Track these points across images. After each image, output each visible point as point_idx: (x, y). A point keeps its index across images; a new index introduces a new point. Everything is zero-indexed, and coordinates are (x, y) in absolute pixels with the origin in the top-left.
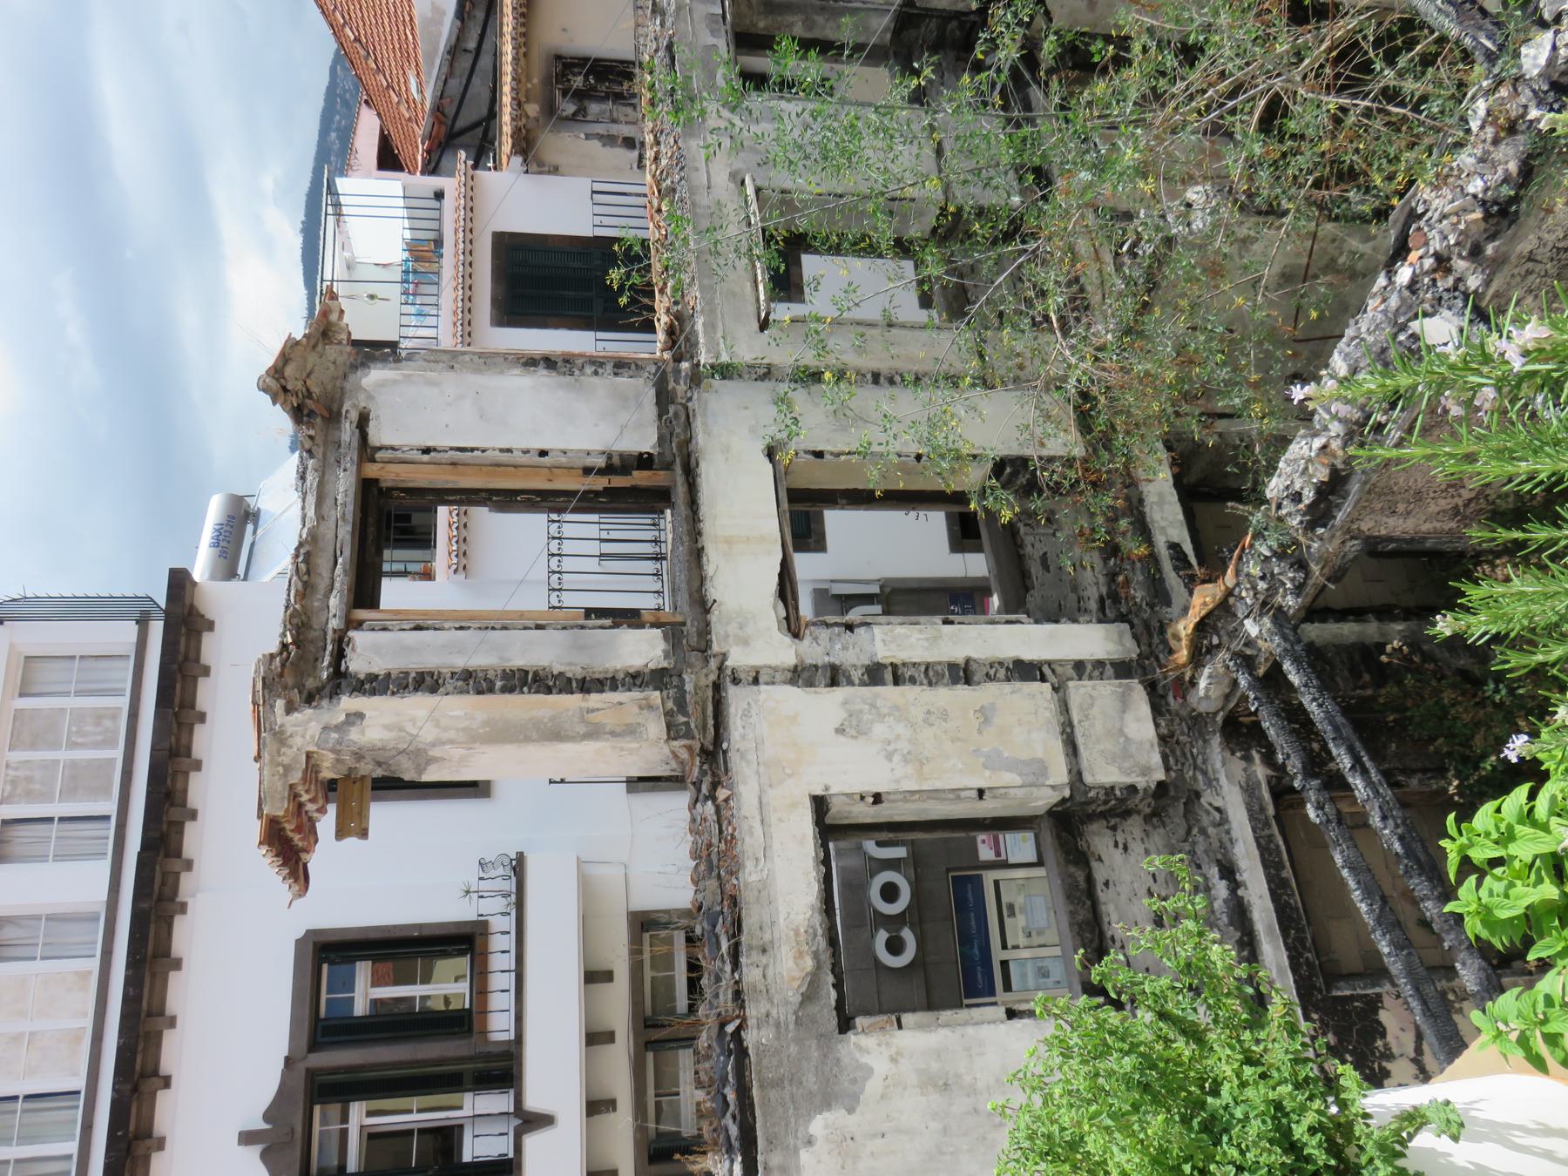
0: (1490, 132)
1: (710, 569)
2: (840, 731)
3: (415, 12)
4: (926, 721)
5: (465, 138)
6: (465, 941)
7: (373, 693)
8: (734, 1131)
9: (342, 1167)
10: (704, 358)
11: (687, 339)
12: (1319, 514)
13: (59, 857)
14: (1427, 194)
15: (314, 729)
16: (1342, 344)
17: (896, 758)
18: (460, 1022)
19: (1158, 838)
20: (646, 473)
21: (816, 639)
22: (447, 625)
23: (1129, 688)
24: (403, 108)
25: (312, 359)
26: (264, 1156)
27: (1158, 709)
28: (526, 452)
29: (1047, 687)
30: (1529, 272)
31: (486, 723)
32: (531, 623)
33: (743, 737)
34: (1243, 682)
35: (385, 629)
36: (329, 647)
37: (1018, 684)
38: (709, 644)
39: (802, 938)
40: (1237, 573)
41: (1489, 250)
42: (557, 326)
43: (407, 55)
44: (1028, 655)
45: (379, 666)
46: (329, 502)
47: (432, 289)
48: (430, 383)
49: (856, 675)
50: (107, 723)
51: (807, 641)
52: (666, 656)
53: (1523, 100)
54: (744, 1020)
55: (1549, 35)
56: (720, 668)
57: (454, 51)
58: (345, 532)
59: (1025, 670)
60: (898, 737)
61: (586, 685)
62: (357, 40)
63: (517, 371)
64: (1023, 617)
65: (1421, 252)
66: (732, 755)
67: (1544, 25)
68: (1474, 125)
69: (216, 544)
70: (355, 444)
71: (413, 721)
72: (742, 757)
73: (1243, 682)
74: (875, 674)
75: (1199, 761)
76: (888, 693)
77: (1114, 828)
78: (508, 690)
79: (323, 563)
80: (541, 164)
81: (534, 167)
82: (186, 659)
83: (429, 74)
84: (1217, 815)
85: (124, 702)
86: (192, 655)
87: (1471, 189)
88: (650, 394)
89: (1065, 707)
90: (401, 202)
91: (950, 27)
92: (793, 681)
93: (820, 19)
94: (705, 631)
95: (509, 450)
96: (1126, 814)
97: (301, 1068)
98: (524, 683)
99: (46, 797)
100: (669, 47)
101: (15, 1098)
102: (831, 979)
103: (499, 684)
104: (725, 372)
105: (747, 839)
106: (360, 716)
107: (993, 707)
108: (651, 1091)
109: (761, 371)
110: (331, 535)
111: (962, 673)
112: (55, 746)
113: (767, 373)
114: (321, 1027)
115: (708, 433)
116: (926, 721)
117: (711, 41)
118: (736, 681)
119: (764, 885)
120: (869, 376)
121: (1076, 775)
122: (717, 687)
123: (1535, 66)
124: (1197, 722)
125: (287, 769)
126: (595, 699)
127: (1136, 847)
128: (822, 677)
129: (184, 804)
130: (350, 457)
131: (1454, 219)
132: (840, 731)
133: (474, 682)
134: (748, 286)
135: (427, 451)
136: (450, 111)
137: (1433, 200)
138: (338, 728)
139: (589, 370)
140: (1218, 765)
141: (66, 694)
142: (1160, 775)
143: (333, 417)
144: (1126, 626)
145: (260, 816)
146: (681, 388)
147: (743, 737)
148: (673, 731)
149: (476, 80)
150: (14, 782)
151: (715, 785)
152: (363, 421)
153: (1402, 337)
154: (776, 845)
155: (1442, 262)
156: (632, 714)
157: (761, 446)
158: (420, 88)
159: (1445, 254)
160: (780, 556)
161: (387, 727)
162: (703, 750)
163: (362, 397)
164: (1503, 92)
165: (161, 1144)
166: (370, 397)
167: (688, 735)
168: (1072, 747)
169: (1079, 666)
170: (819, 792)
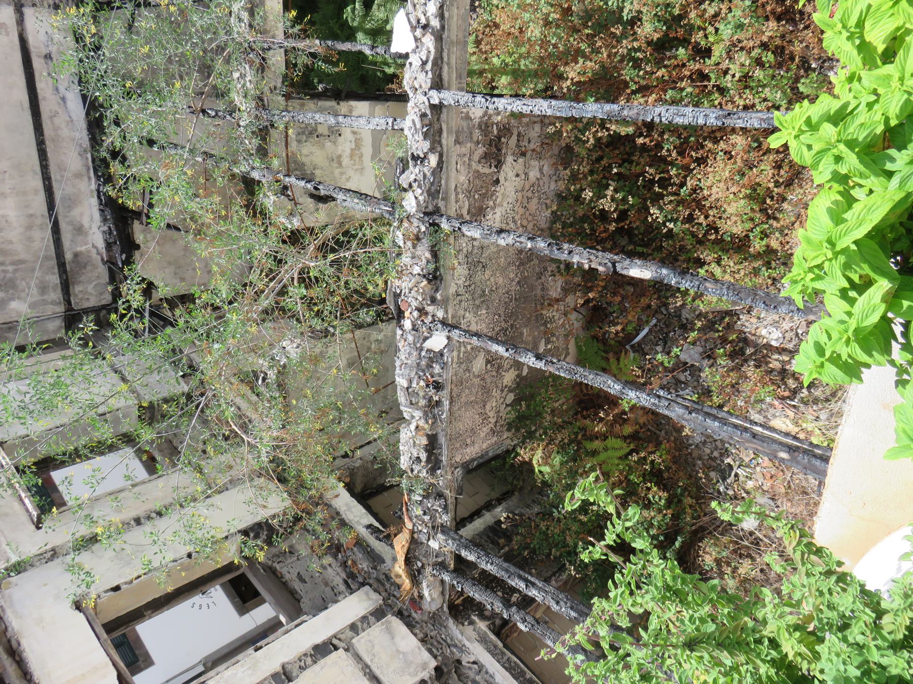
0: (409, 244)
12: (434, 464)
14: (397, 283)
16: (397, 371)
23: (389, 622)
27: (410, 624)
29: (341, 651)
30: (461, 301)
34: (447, 578)
40: (411, 519)
41: (438, 296)
44: (319, 639)
53: (416, 224)
55: (410, 193)
59: (323, 650)
64: (304, 617)
65: (409, 310)
67: (405, 190)
68: (401, 243)
73: (447, 578)
75: (449, 641)
84: (475, 666)
87: (415, 272)
89: (358, 658)
91: (101, 314)
109: (49, 555)
113: (54, 553)
120: (132, 522)
123: (412, 207)
124: (435, 618)
131: (416, 289)
134: (17, 506)
137: (403, 284)
140: (460, 636)
142: (433, 664)
144: (367, 587)
153: (423, 353)
155: (422, 311)
157: (68, 605)
159: (421, 307)
160: (115, 673)
164: (406, 224)
169: (353, 627)
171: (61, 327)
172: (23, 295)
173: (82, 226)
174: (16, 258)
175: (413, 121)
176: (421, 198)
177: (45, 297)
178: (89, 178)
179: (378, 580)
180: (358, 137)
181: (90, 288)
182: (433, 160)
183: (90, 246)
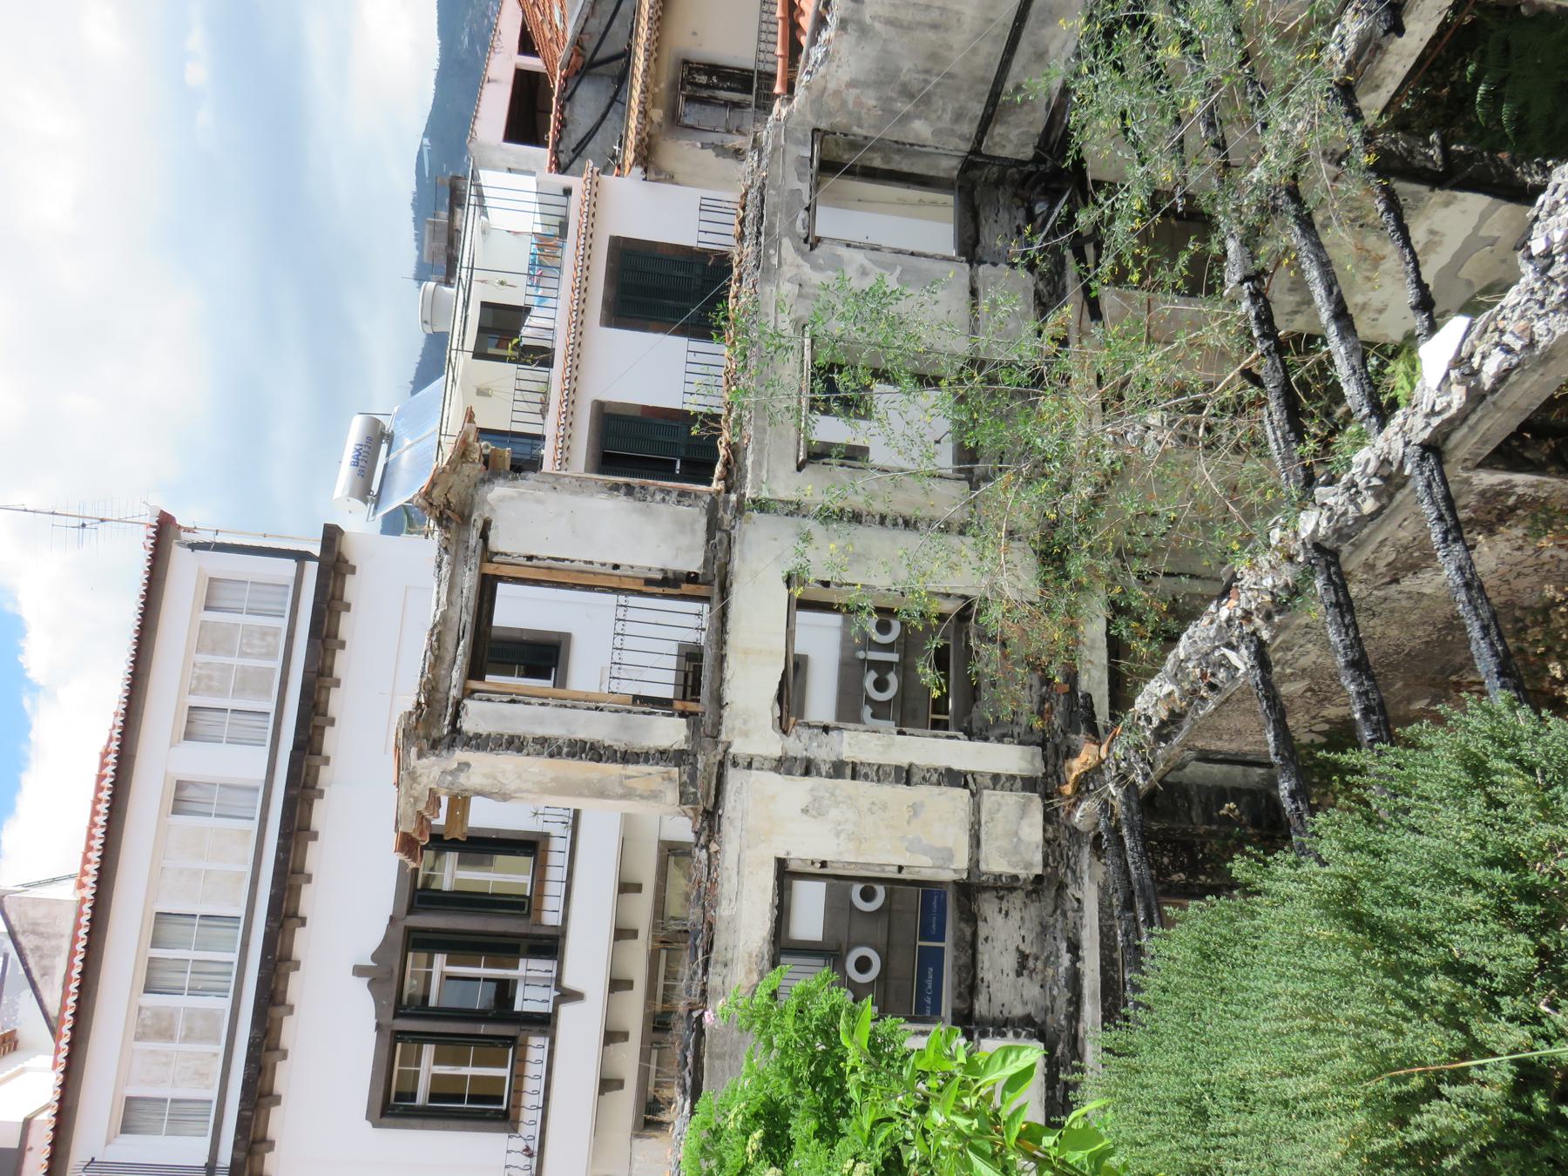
1: (728, 674)
2: (805, 811)
4: (870, 810)
5: (601, 69)
6: (530, 846)
7: (478, 748)
8: (689, 1081)
9: (426, 998)
10: (749, 493)
11: (740, 470)
12: (1163, 733)
15: (436, 772)
17: (843, 836)
18: (521, 905)
19: (1033, 910)
20: (692, 587)
24: (546, 27)
25: (454, 478)
26: (370, 985)
27: (1049, 817)
28: (603, 565)
31: (553, 780)
32: (592, 705)
33: (734, 808)
35: (489, 700)
36: (450, 710)
37: (944, 789)
38: (719, 732)
39: (754, 959)
40: (1109, 750)
41: (1277, 619)
42: (656, 331)
44: (957, 766)
45: (484, 729)
46: (457, 591)
48: (539, 501)
49: (824, 768)
50: (270, 639)
51: (791, 738)
52: (687, 741)
58: (467, 618)
59: (953, 778)
61: (628, 757)
63: (603, 496)
64: (960, 734)
69: (356, 464)
70: (479, 551)
72: (731, 823)
74: (839, 769)
76: (846, 785)
77: (1001, 898)
78: (571, 755)
80: (659, 171)
81: (652, 175)
82: (333, 598)
85: (284, 623)
86: (338, 593)
88: (703, 522)
89: (977, 809)
90: (534, 197)
92: (776, 770)
93: (897, 158)
95: (591, 563)
96: (1011, 889)
97: (401, 926)
98: (583, 750)
99: (222, 692)
101: (194, 916)
103: (565, 750)
104: (762, 506)
105: (726, 885)
106: (467, 765)
107: (922, 805)
109: (792, 508)
110: (456, 619)
111: (905, 776)
112: (230, 653)
113: (795, 509)
115: (743, 560)
116: (870, 810)
117: (798, 185)
118: (735, 764)
119: (733, 918)
121: (975, 862)
122: (721, 764)
124: (1075, 833)
125: (416, 800)
126: (632, 769)
127: (1015, 915)
128: (799, 768)
129: (325, 714)
130: (474, 561)
132: (805, 811)
133: (548, 747)
134: (793, 432)
135: (530, 558)
136: (590, 46)
138: (451, 773)
139: (658, 497)
140: (1085, 867)
141: (238, 611)
142: (1039, 870)
143: (465, 520)
145: (397, 830)
146: (728, 517)
147: (734, 808)
148: (684, 797)
149: (616, 23)
150: (199, 678)
152: (487, 525)
155: (1247, 615)
161: (486, 776)
162: (705, 811)
163: (487, 508)
165: (297, 966)
166: (492, 510)
167: (695, 802)
168: (976, 841)
169: (996, 778)
170: (782, 856)
171: (954, 168)
172: (933, 116)
173: (1046, 52)
175: (1368, 461)
176: (1322, 531)
177: (956, 127)
179: (1056, 747)
180: (1437, 239)
181: (1014, 134)
182: (1369, 506)
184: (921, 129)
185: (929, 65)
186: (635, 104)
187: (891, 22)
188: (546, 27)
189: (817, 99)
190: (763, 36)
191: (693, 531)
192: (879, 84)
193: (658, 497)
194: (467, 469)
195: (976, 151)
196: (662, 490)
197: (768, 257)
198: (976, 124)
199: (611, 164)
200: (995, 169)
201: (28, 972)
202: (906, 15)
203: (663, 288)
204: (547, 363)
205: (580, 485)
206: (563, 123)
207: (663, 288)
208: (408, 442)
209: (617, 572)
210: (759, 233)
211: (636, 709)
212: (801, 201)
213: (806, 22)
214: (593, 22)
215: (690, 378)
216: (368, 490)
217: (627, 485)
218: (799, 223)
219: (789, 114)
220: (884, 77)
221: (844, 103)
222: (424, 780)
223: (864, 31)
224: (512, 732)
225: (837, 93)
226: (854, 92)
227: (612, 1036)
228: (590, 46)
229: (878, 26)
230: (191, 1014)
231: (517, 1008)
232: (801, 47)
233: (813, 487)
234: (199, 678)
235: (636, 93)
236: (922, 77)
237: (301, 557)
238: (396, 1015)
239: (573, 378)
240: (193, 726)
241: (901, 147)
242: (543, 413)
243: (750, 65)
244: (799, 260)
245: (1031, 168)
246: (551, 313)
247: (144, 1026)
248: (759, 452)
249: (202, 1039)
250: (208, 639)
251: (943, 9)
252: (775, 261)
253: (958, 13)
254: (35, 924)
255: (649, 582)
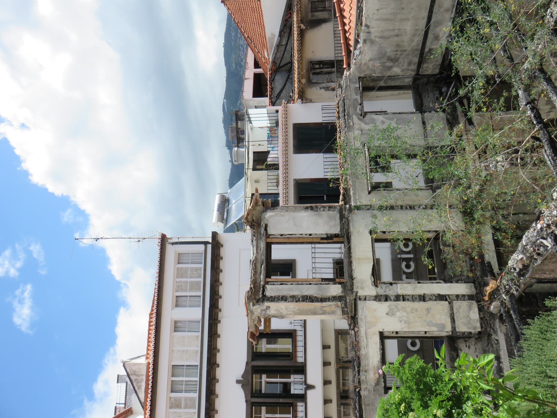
1: (354, 268)
2: (387, 314)
3: (267, 38)
4: (411, 312)
5: (282, 69)
6: (290, 335)
7: (272, 301)
8: (358, 414)
9: (261, 390)
10: (353, 204)
11: (348, 196)
12: (521, 273)
13: (190, 306)
15: (259, 310)
17: (402, 322)
18: (290, 356)
19: (479, 345)
20: (337, 239)
21: (382, 287)
22: (288, 283)
23: (472, 303)
24: (263, 59)
25: (254, 212)
26: (242, 386)
27: (481, 309)
28: (306, 235)
29: (447, 302)
31: (298, 310)
32: (308, 283)
33: (362, 315)
34: (502, 310)
36: (261, 289)
37: (438, 302)
38: (353, 288)
39: (376, 369)
40: (501, 282)
42: (312, 153)
43: (264, 45)
44: (442, 293)
45: (273, 294)
46: (259, 249)
47: (276, 142)
48: (282, 216)
49: (392, 298)
50: (198, 271)
52: (342, 292)
54: (361, 389)
56: (356, 295)
57: (279, 46)
58: (264, 258)
60: (403, 316)
61: (322, 300)
62: (248, 37)
66: (359, 320)
69: (218, 211)
71: (281, 309)
73: (502, 310)
74: (398, 298)
75: (492, 326)
76: (401, 303)
77: (466, 341)
78: (303, 301)
79: (259, 265)
80: (307, 99)
81: (305, 101)
83: (271, 49)
84: (496, 342)
85: (202, 266)
89: (452, 308)
90: (266, 115)
92: (375, 300)
93: (389, 81)
94: (352, 285)
96: (470, 338)
97: (250, 365)
98: (307, 299)
99: (185, 291)
100: (344, 100)
102: (383, 380)
103: (301, 299)
104: (358, 208)
105: (362, 343)
106: (269, 307)
107: (430, 308)
108: (341, 381)
109: (368, 207)
110: (260, 258)
111: (423, 298)
112: (187, 277)
113: (370, 208)
114: (254, 355)
115: (354, 227)
116: (411, 312)
117: (356, 97)
118: (360, 299)
119: (366, 355)
121: (454, 328)
122: (355, 300)
124: (492, 314)
125: (254, 320)
126: (324, 304)
127: (473, 347)
128: (383, 299)
132: (387, 314)
133: (295, 299)
134: (365, 181)
135: (282, 235)
136: (278, 62)
138: (265, 310)
139: (322, 209)
140: (498, 327)
141: (188, 263)
142: (479, 330)
143: (259, 225)
144: (473, 284)
146: (346, 213)
147: (362, 315)
148: (344, 313)
149: (286, 53)
150: (178, 287)
151: (354, 326)
152: (266, 226)
154: (370, 345)
155: (548, 226)
156: (333, 308)
158: (268, 56)
160: (372, 264)
161: (276, 310)
162: (352, 317)
165: (218, 381)
166: (267, 220)
167: (348, 314)
168: (453, 320)
169: (457, 296)
171: (410, 82)
172: (400, 65)
173: (439, 36)
174: (403, 49)
177: (409, 67)
178: (452, 12)
179: (479, 283)
181: (431, 66)
183: (439, 46)
184: (396, 70)
185: (397, 49)
186: (296, 79)
187: (381, 37)
188: (263, 59)
189: (359, 67)
190: (336, 48)
191: (335, 219)
192: (380, 58)
193: (322, 209)
194: (258, 208)
195: (417, 74)
196: (323, 207)
197: (349, 123)
198: (416, 65)
199: (290, 100)
200: (425, 79)
201: (134, 388)
202: (386, 34)
203: (313, 138)
204: (277, 169)
205: (295, 210)
206: (272, 89)
207: (313, 138)
208: (234, 201)
209: (311, 236)
210: (345, 115)
211: (323, 283)
212: (358, 102)
213: (352, 43)
214: (278, 54)
215: (326, 167)
216: (223, 219)
217: (311, 207)
218: (358, 109)
219: (350, 74)
220: (382, 56)
221: (368, 67)
222: (256, 313)
223: (372, 42)
224: (282, 295)
225: (365, 64)
226: (371, 62)
227: (327, 401)
228: (278, 62)
229: (377, 39)
230: (186, 399)
231: (292, 392)
232: (351, 51)
233: (375, 199)
234: (178, 287)
235: (296, 75)
236: (395, 53)
237: (206, 243)
238: (252, 397)
239: (286, 173)
240: (178, 303)
241: (390, 78)
242: (277, 186)
243: (333, 59)
244: (360, 122)
245: (439, 76)
246: (276, 152)
247: (172, 404)
248: (354, 190)
249: (190, 407)
250: (180, 273)
251: (399, 29)
252: (351, 124)
253: (405, 29)
254: (135, 372)
255: (322, 239)
